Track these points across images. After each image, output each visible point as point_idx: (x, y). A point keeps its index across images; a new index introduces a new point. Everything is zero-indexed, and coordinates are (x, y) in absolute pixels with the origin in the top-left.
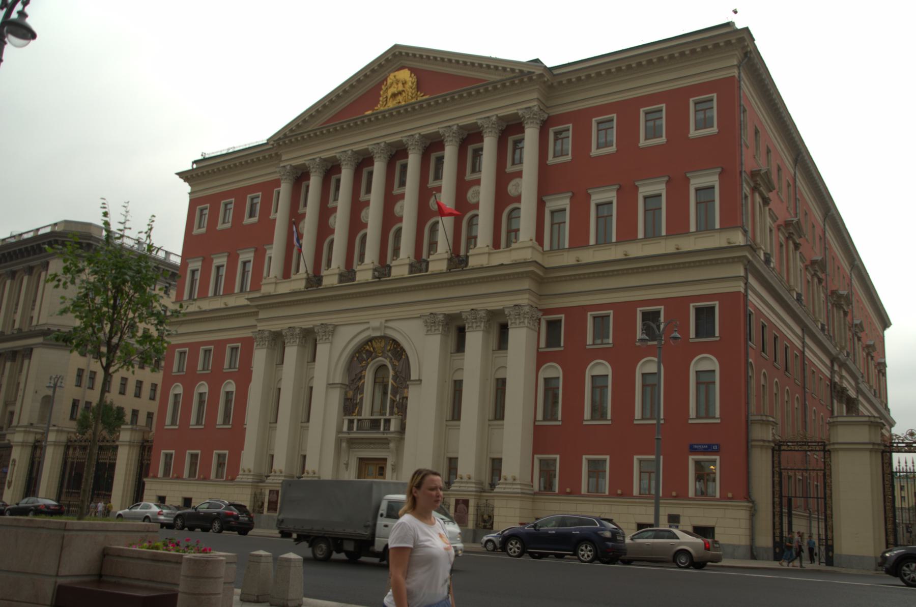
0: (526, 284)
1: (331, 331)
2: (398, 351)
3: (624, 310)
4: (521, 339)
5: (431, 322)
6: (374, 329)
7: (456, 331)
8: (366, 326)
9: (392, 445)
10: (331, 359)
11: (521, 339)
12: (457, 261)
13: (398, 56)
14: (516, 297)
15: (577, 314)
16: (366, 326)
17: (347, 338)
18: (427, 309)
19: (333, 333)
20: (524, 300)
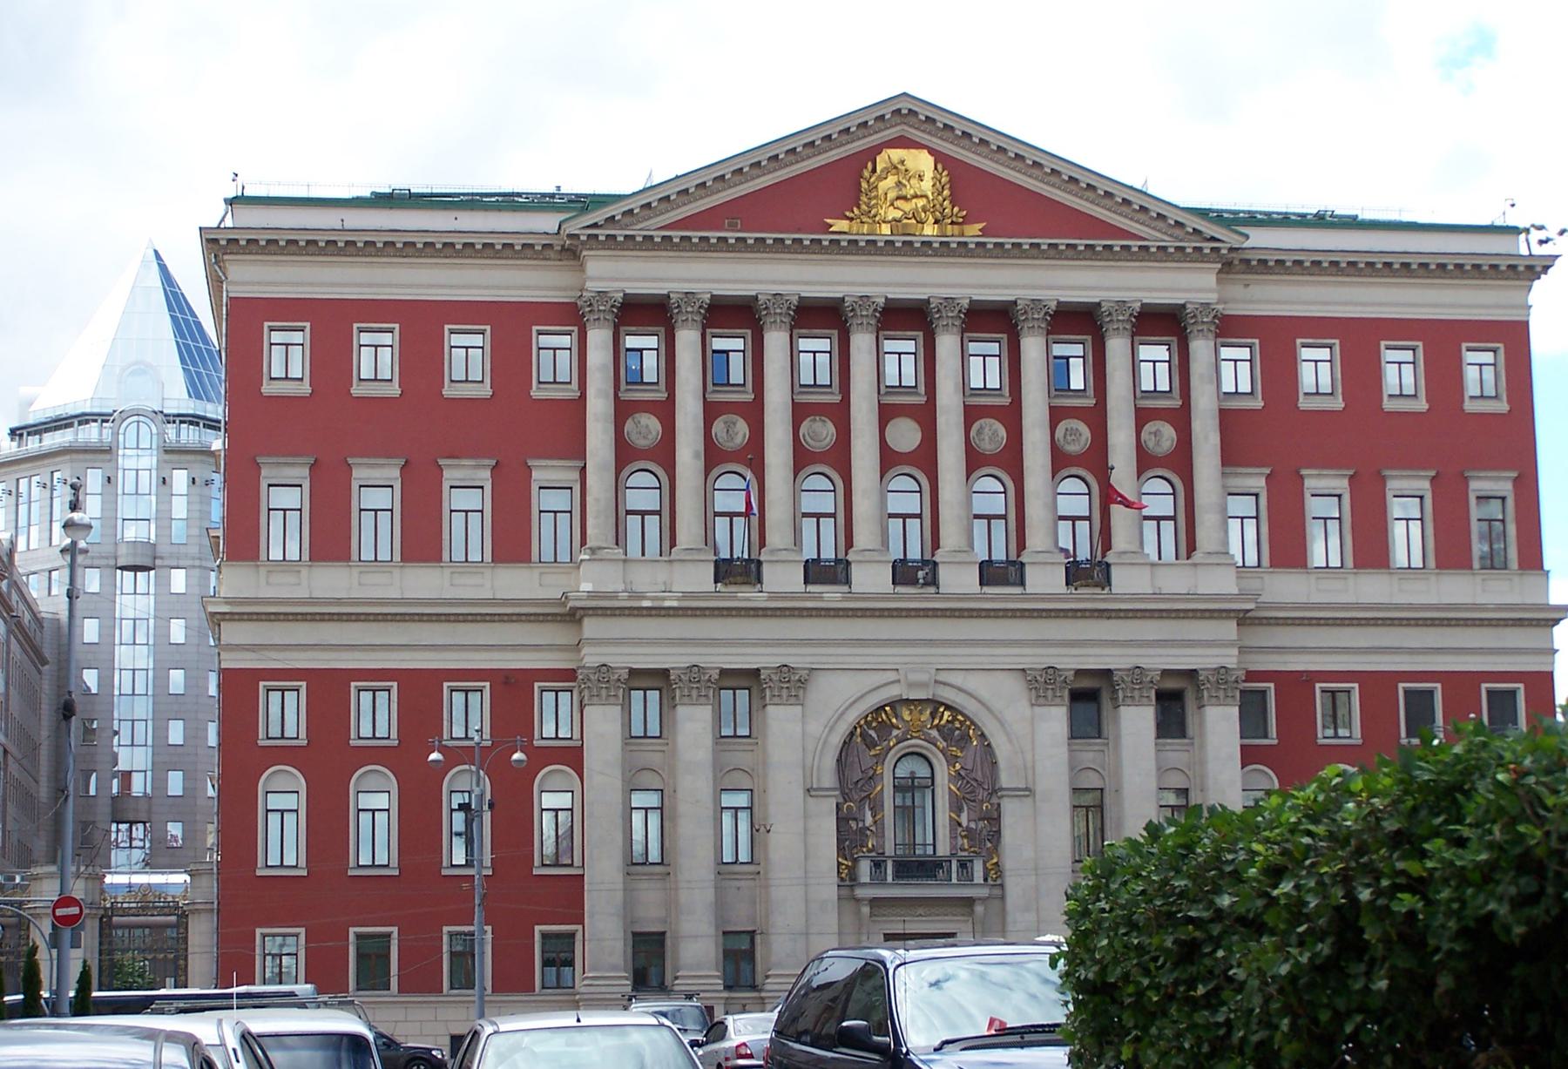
0: (1229, 629)
1: (793, 683)
2: (960, 732)
3: (1377, 685)
4: (1220, 726)
5: (1041, 683)
6: (911, 685)
7: (1089, 698)
8: (892, 676)
9: (979, 909)
10: (800, 740)
11: (1220, 726)
12: (1087, 573)
13: (905, 120)
14: (1211, 649)
15: (1296, 685)
16: (892, 676)
17: (841, 698)
18: (1037, 659)
19: (803, 683)
20: (1230, 658)
